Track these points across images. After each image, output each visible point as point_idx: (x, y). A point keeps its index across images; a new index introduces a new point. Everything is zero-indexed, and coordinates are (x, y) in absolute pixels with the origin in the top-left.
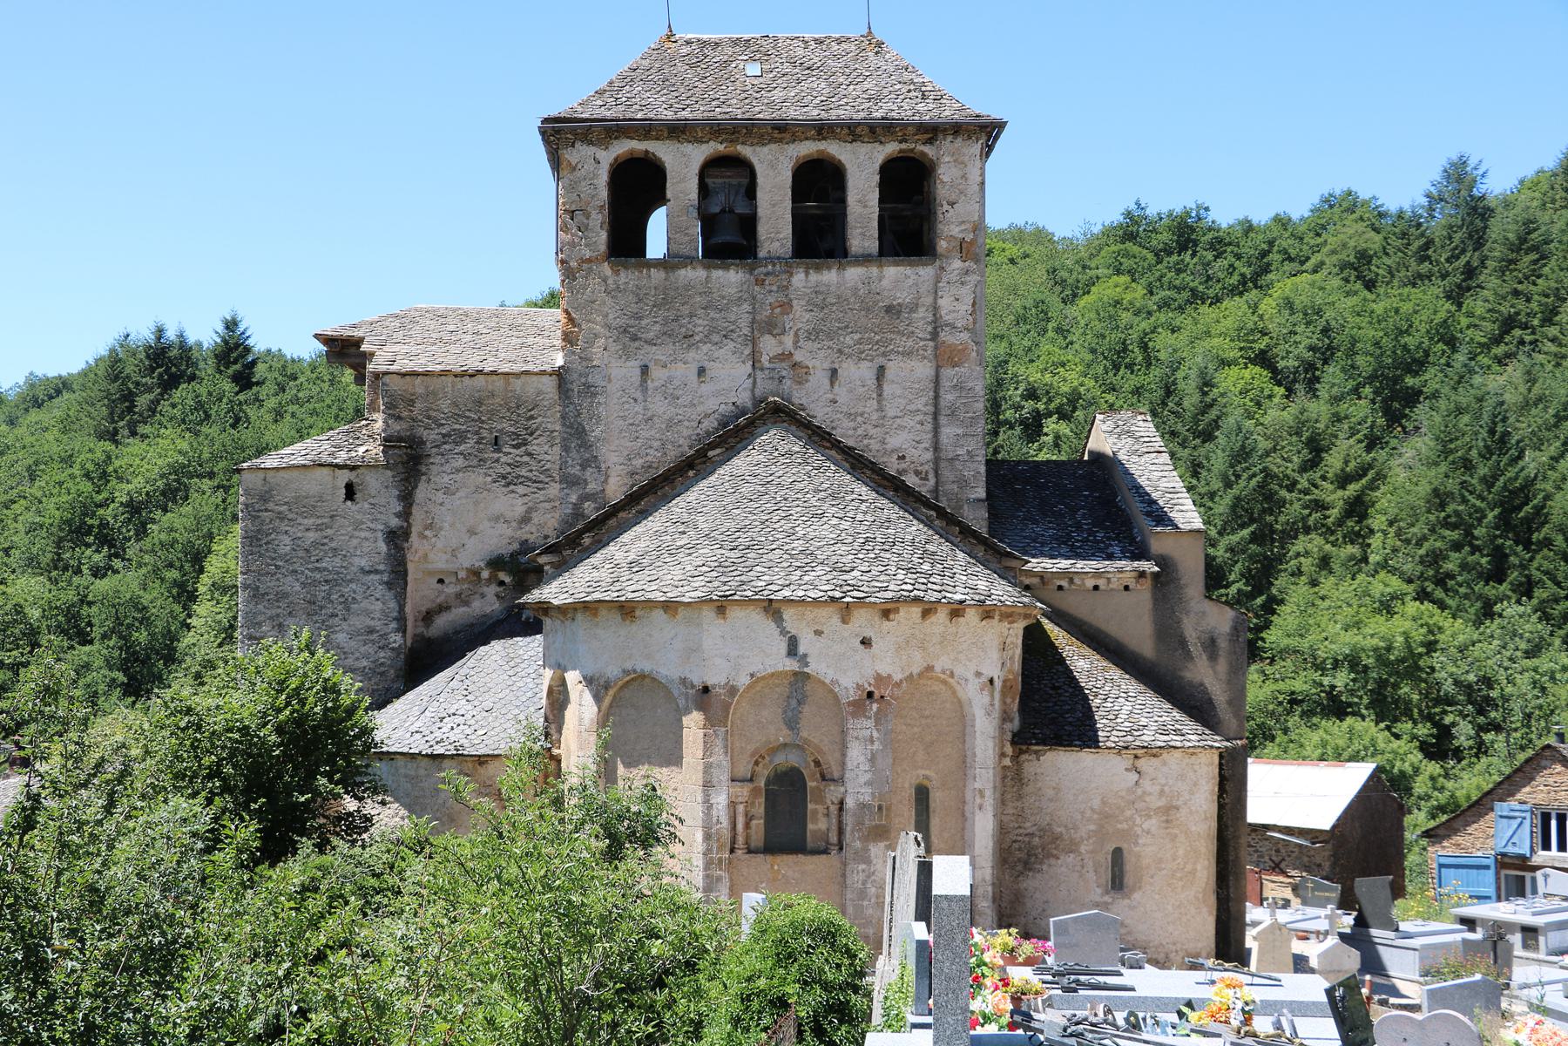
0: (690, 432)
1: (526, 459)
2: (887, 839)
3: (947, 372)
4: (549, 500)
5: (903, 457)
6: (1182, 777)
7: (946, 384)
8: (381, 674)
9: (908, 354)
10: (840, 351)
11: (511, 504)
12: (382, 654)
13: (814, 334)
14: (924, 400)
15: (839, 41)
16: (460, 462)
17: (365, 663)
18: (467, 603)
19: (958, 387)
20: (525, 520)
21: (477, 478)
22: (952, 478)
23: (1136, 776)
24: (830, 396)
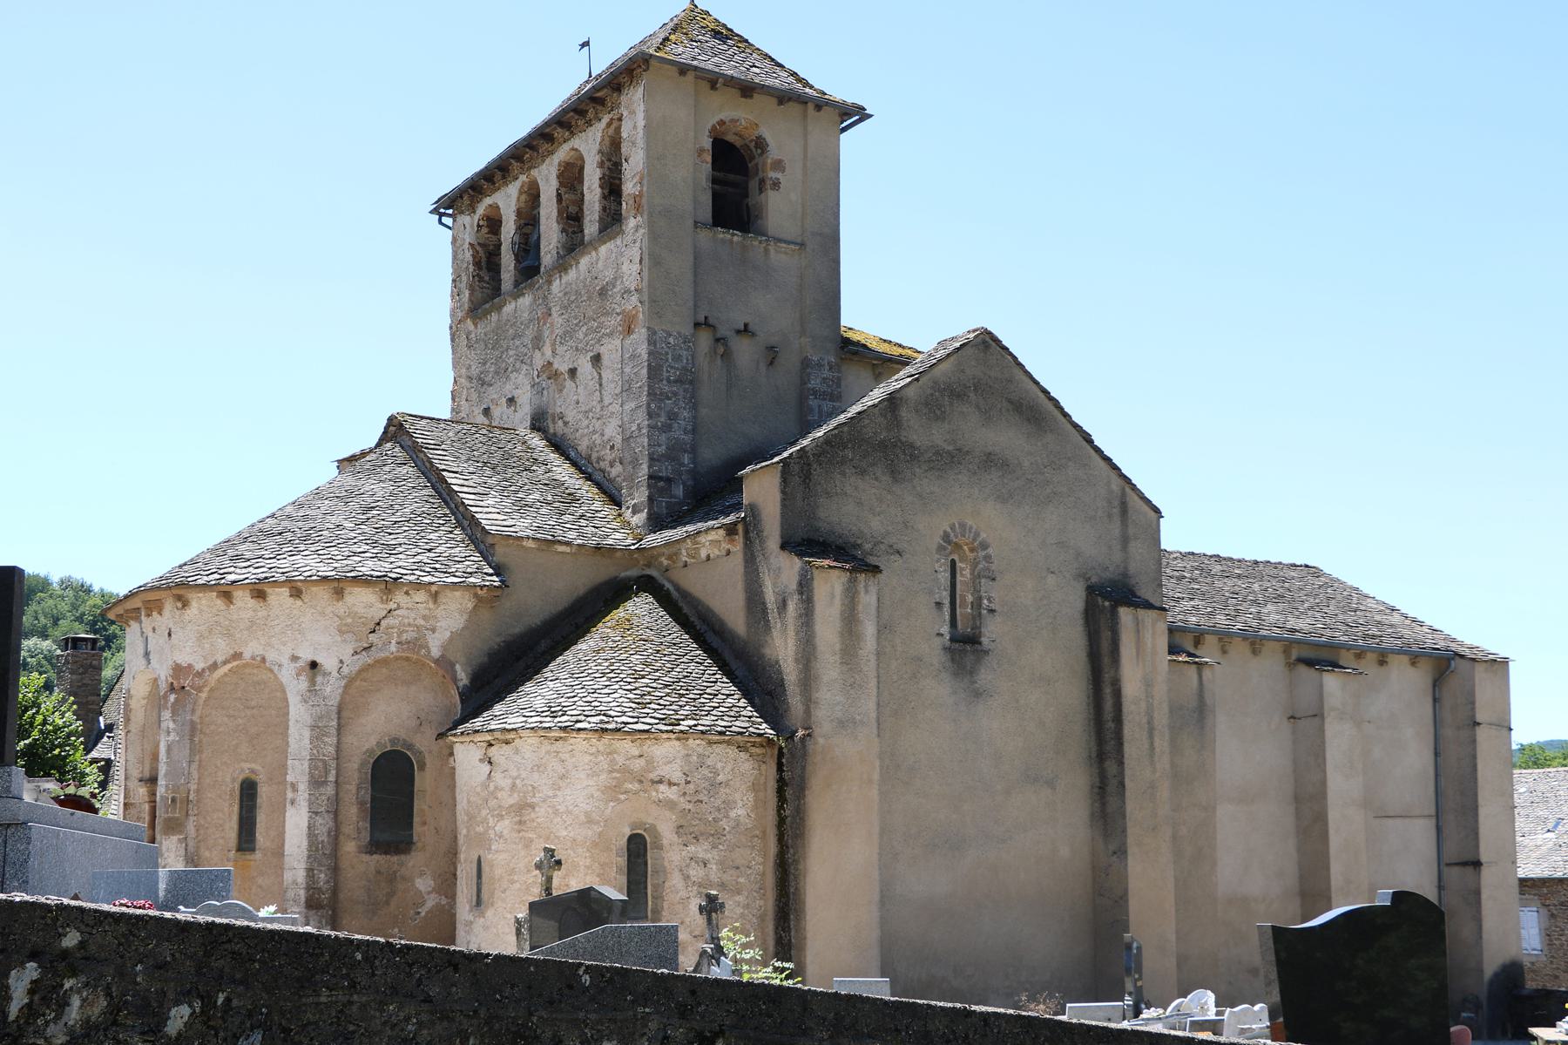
2: (180, 832)
5: (612, 447)
6: (539, 768)
19: (633, 357)
23: (487, 768)
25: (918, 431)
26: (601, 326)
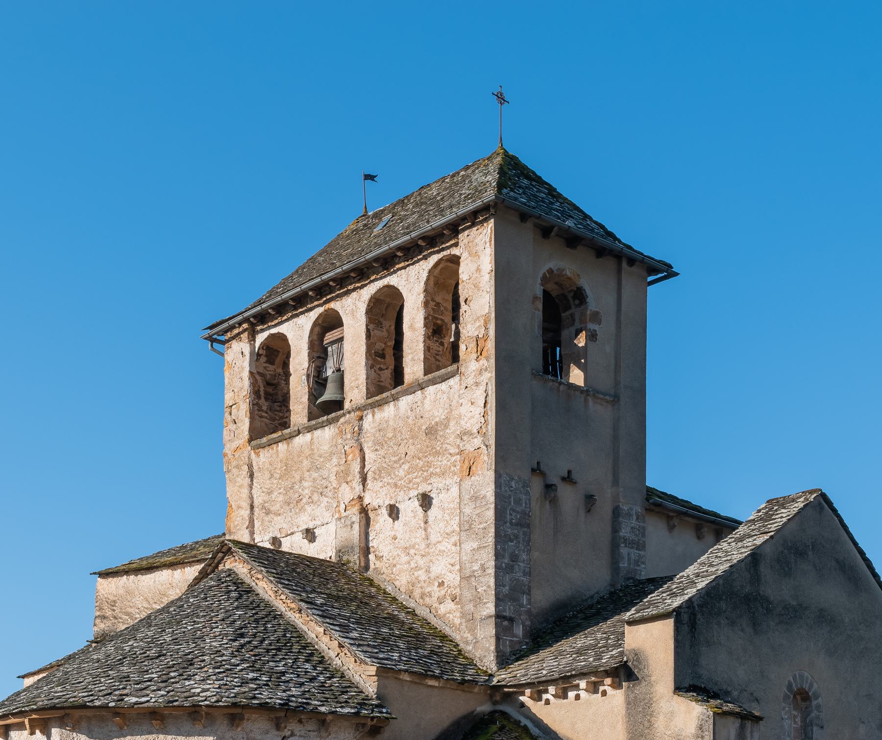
3: (467, 483)
5: (441, 584)
10: (396, 485)
19: (475, 498)
25: (776, 589)
26: (429, 465)
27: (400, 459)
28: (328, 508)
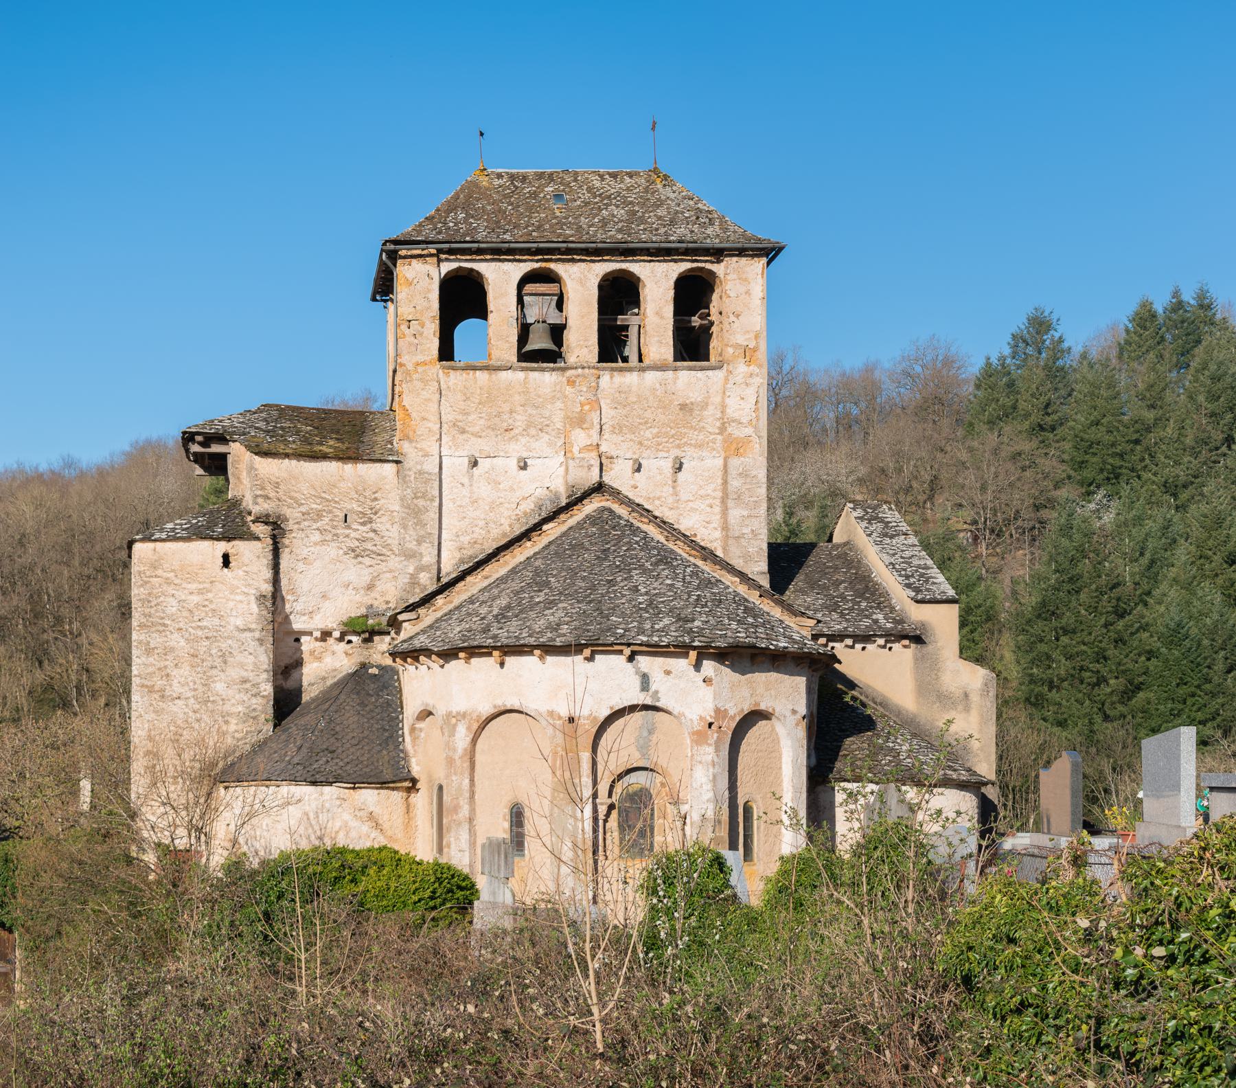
0: (510, 513)
1: (372, 535)
3: (734, 462)
4: (391, 571)
7: (733, 472)
8: (254, 718)
9: (699, 446)
10: (640, 443)
11: (357, 573)
12: (254, 701)
13: (618, 429)
14: (712, 486)
15: (630, 175)
16: (316, 537)
17: (240, 708)
18: (319, 659)
19: (744, 475)
20: (370, 587)
21: (332, 551)
22: (738, 553)
24: (633, 483)
26: (683, 435)
27: (646, 423)
28: (550, 444)
